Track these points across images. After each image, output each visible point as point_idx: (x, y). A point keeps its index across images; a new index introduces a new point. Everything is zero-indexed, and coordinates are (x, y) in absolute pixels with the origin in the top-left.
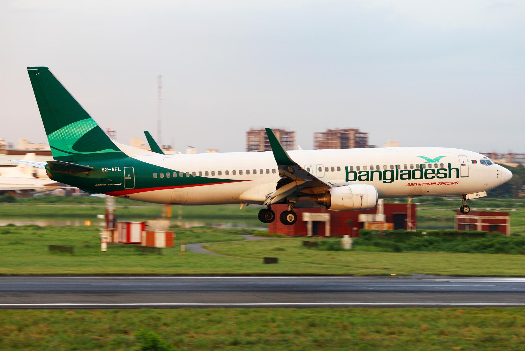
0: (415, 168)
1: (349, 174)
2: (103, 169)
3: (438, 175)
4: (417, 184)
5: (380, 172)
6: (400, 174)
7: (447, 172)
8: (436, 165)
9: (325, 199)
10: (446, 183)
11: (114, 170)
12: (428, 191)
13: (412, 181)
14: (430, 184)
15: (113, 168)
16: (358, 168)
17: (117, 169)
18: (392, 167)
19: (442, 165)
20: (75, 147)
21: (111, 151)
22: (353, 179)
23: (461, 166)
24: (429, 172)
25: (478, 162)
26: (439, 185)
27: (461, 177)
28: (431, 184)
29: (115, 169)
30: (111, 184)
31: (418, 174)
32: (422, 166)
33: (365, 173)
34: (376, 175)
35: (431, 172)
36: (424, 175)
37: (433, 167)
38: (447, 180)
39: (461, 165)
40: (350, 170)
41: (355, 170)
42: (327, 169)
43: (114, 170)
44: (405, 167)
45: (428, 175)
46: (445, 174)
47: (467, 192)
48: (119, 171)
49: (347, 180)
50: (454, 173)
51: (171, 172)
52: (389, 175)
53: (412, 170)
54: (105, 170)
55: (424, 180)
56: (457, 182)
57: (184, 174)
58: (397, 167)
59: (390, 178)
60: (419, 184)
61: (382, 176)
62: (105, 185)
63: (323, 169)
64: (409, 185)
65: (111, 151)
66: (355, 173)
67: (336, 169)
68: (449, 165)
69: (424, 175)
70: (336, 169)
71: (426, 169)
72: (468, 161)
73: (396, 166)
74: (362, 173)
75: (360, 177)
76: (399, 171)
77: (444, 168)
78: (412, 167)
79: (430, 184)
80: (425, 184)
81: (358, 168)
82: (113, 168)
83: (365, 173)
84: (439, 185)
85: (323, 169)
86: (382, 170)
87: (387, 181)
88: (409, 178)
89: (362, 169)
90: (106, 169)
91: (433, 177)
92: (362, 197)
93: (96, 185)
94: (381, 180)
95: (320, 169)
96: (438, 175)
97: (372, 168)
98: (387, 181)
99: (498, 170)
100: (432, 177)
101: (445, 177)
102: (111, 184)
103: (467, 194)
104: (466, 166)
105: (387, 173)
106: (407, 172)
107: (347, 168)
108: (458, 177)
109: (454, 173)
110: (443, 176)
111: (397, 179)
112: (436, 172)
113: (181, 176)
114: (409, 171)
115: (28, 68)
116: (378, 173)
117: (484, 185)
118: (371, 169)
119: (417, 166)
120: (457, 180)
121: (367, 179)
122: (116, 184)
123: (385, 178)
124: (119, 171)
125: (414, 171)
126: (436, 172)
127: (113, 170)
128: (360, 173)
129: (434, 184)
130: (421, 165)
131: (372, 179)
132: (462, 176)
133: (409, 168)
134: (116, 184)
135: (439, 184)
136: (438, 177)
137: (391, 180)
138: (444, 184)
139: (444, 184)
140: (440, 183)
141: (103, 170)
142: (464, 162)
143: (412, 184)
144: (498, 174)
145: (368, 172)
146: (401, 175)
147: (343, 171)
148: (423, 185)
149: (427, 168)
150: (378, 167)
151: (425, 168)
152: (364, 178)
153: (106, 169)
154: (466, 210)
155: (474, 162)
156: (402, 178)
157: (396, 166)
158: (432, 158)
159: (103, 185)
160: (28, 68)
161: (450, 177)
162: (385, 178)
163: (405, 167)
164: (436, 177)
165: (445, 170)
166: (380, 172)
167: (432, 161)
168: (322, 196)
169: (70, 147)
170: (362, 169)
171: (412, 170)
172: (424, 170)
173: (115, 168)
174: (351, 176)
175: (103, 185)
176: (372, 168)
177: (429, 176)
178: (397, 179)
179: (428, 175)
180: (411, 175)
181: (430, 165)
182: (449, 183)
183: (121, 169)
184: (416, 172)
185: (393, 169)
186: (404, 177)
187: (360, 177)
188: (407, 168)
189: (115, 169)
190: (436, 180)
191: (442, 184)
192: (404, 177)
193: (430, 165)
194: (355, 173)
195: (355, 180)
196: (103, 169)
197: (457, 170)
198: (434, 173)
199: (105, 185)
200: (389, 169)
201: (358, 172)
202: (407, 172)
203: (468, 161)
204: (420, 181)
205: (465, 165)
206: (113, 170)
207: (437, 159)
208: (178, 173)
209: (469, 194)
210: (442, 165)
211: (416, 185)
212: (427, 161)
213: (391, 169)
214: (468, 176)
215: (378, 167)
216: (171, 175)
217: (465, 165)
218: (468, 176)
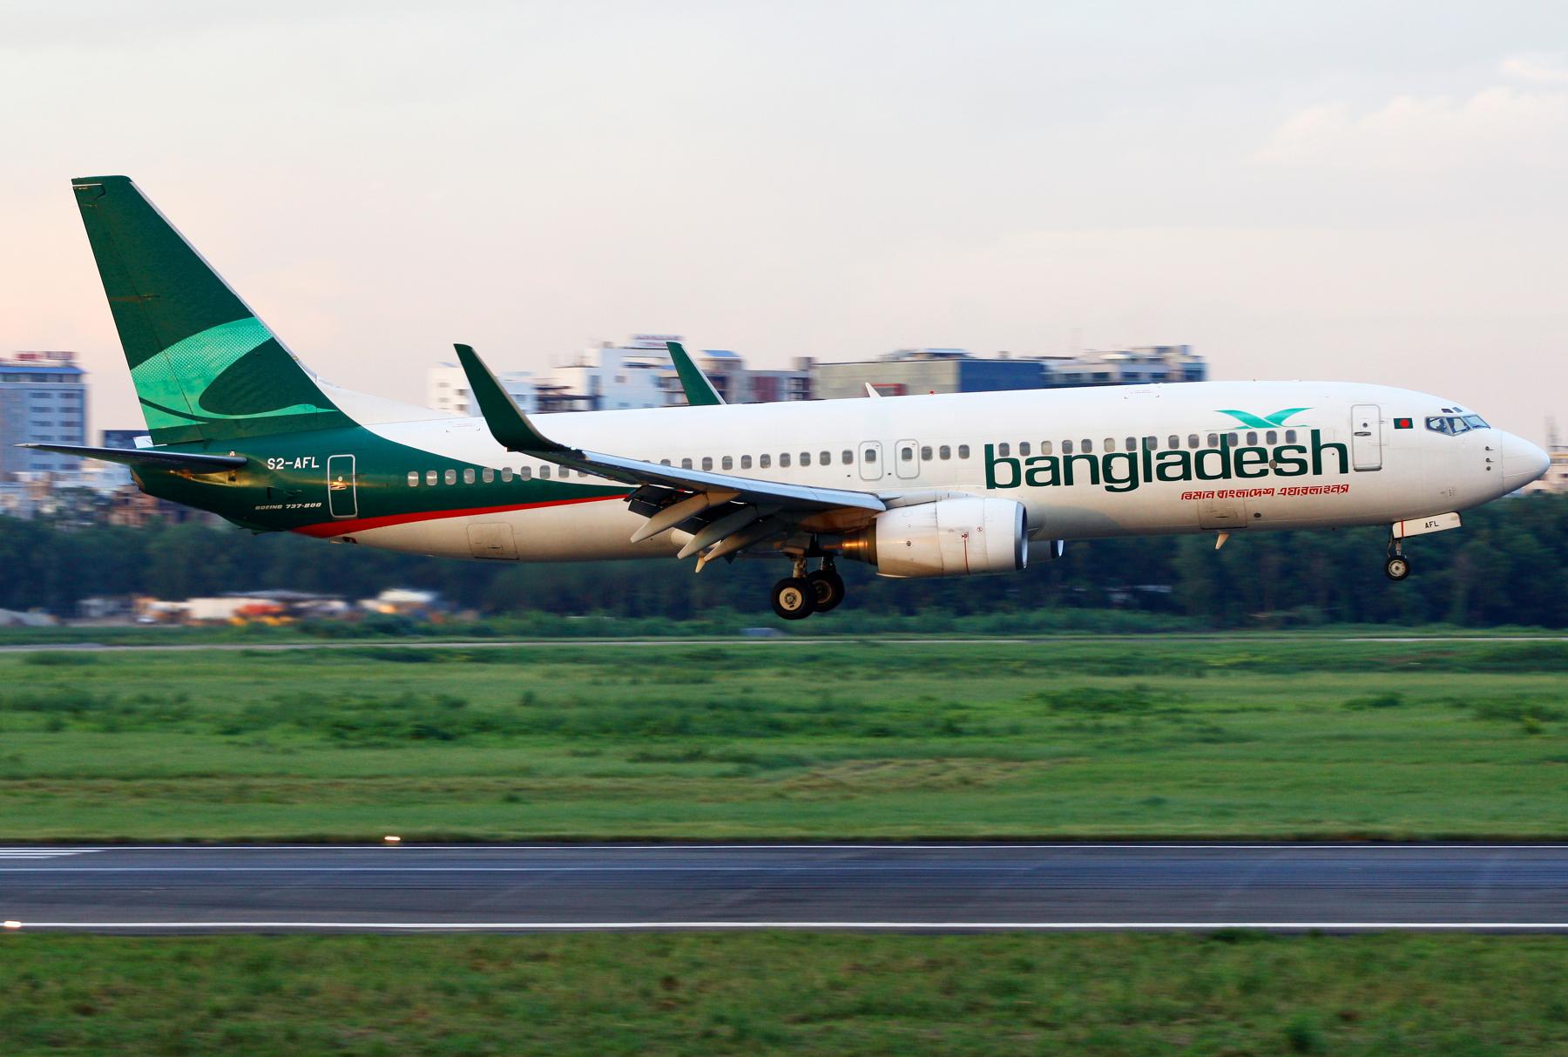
0: (1204, 446)
1: (997, 467)
2: (271, 461)
3: (1279, 466)
4: (1216, 494)
5: (1093, 460)
6: (1155, 463)
7: (1308, 457)
8: (1271, 437)
10: (1306, 490)
11: (302, 465)
12: (1258, 515)
13: (1196, 484)
14: (1256, 494)
15: (298, 459)
16: (1025, 447)
17: (310, 461)
18: (1131, 442)
19: (1291, 435)
20: (205, 402)
21: (311, 409)
22: (1009, 480)
23: (1355, 437)
24: (1247, 456)
25: (1419, 424)
26: (1284, 494)
27: (1356, 470)
28: (1258, 492)
29: (305, 462)
30: (294, 506)
31: (1213, 464)
32: (1227, 440)
33: (1047, 463)
34: (1081, 468)
35: (1255, 456)
36: (1233, 465)
37: (1262, 442)
38: (1309, 479)
39: (1356, 434)
40: (1001, 454)
41: (1014, 453)
42: (927, 454)
43: (302, 465)
44: (1174, 442)
45: (1244, 465)
46: (1302, 464)
47: (1397, 517)
48: (313, 466)
49: (991, 483)
50: (1330, 458)
51: (460, 466)
52: (1120, 469)
53: (1193, 453)
54: (276, 464)
55: (1235, 482)
56: (1345, 487)
57: (497, 473)
58: (1149, 443)
59: (1127, 475)
60: (1222, 494)
61: (1101, 470)
62: (280, 507)
63: (916, 453)
64: (1187, 496)
65: (311, 409)
66: (1015, 464)
67: (955, 452)
68: (1315, 434)
69: (1233, 465)
70: (955, 452)
71: (1238, 447)
72: (1381, 422)
73: (1144, 440)
74: (1037, 464)
75: (1030, 474)
76: (1154, 454)
77: (1297, 444)
78: (1194, 442)
79: (1256, 494)
80: (1241, 493)
81: (1025, 447)
82: (298, 459)
83: (1047, 463)
84: (1284, 494)
85: (916, 453)
86: (1099, 452)
87: (1117, 486)
88: (1186, 476)
89: (1036, 451)
90: (280, 461)
91: (1264, 473)
92: (965, 536)
93: (257, 508)
94: (1098, 483)
95: (907, 454)
96: (1279, 466)
97: (1067, 446)
98: (1117, 486)
99: (1487, 449)
100: (1258, 471)
101: (1303, 469)
102: (294, 506)
103: (1394, 523)
104: (1374, 438)
105: (1115, 462)
106: (1178, 458)
107: (989, 449)
108: (1344, 468)
109: (1330, 458)
110: (1295, 467)
111: (1148, 478)
112: (1270, 457)
113: (488, 479)
114: (1186, 455)
115: (74, 181)
116: (1086, 463)
117: (1442, 493)
118: (1064, 451)
119: (1212, 439)
120: (1342, 479)
121: (1055, 481)
122: (307, 506)
123: (1109, 478)
124: (313, 466)
125: (1200, 456)
126: (1270, 457)
127: (298, 464)
128: (1029, 462)
129: (1270, 491)
130: (1223, 436)
131: (1069, 481)
132: (1358, 467)
133: (1184, 446)
134: (307, 506)
135: (1284, 492)
136: (1279, 472)
137: (1128, 484)
138: (1301, 493)
139: (1301, 493)
140: (1288, 491)
141: (271, 466)
142: (1365, 425)
143: (1199, 494)
144: (1488, 460)
145: (1054, 461)
146: (1161, 468)
147: (978, 458)
148: (1235, 495)
149: (1242, 443)
150: (1087, 444)
151: (1235, 443)
152: (1045, 476)
153: (280, 461)
154: (1397, 568)
155: (1403, 423)
156: (1162, 476)
157: (1144, 439)
158: (1261, 415)
159: (275, 507)
160: (74, 181)
161: (1318, 470)
162: (1109, 478)
163: (1174, 442)
164: (1271, 471)
165: (1302, 450)
166: (1093, 460)
167: (1258, 423)
169: (194, 398)
170: (1036, 451)
171: (1193, 453)
172: (1232, 450)
173: (305, 458)
174: (1003, 473)
175: (275, 507)
176: (1067, 446)
177: (1247, 469)
178: (1148, 478)
179: (1244, 465)
180: (1192, 466)
181: (1252, 437)
182: (1315, 490)
183: (321, 461)
184: (1207, 457)
185: (1135, 449)
186: (1170, 471)
187: (1030, 474)
188: (1177, 446)
189: (305, 462)
190: (1272, 480)
191: (1293, 491)
192: (1170, 471)
193: (1252, 437)
194: (1015, 464)
195: (1016, 483)
196: (271, 461)
197: (1342, 449)
198: (1264, 458)
199: (280, 507)
201: (1022, 460)
202: (1178, 458)
203: (1381, 422)
204: (1222, 484)
205: (1368, 434)
206: (298, 464)
207: (1278, 420)
208: (479, 470)
209: (1402, 521)
210: (1291, 435)
211: (1210, 495)
212: (1243, 424)
213: (1128, 449)
214: (1379, 469)
215: (1087, 444)
216: (460, 477)
217: (1368, 434)
218: (1379, 469)
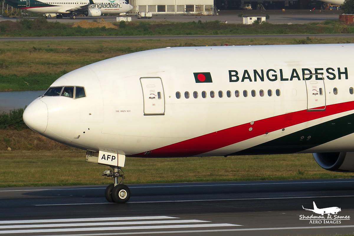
6: (103, 6)
9: (86, 13)
31: (108, 6)
52: (100, 6)
53: (106, 5)
55: (110, 8)
64: (105, 9)
116: (97, 5)
123: (99, 7)
162: (99, 7)
168: (85, 12)
200: (100, 4)
